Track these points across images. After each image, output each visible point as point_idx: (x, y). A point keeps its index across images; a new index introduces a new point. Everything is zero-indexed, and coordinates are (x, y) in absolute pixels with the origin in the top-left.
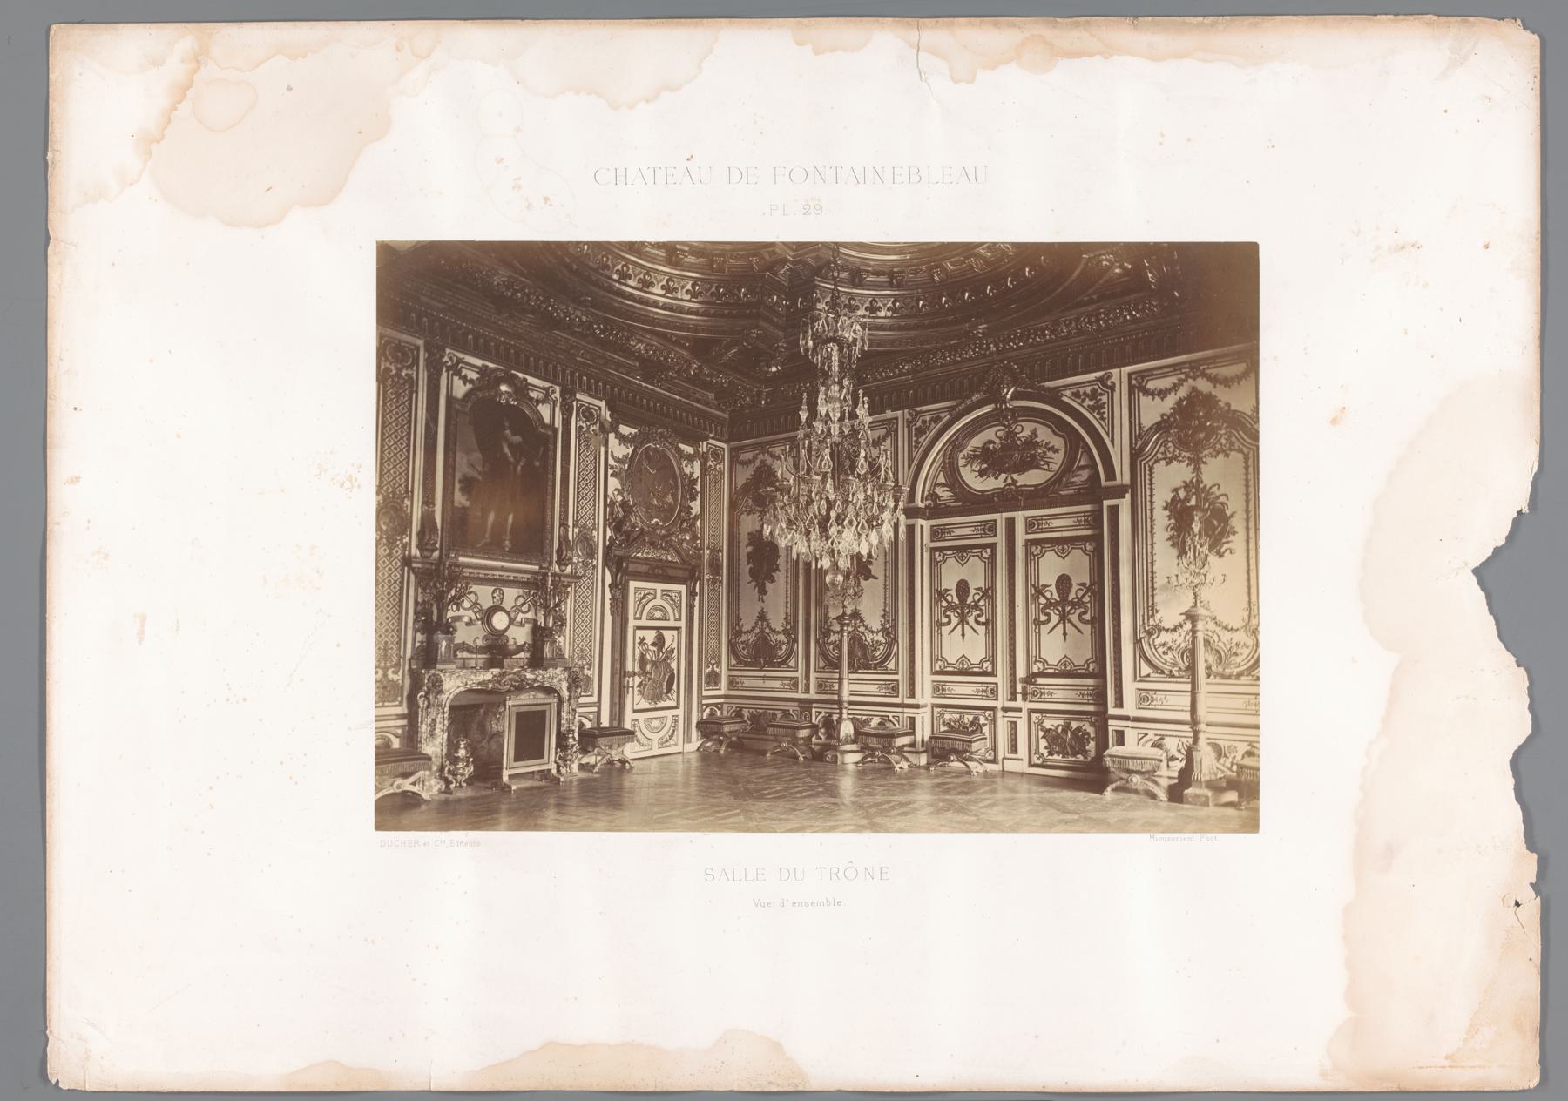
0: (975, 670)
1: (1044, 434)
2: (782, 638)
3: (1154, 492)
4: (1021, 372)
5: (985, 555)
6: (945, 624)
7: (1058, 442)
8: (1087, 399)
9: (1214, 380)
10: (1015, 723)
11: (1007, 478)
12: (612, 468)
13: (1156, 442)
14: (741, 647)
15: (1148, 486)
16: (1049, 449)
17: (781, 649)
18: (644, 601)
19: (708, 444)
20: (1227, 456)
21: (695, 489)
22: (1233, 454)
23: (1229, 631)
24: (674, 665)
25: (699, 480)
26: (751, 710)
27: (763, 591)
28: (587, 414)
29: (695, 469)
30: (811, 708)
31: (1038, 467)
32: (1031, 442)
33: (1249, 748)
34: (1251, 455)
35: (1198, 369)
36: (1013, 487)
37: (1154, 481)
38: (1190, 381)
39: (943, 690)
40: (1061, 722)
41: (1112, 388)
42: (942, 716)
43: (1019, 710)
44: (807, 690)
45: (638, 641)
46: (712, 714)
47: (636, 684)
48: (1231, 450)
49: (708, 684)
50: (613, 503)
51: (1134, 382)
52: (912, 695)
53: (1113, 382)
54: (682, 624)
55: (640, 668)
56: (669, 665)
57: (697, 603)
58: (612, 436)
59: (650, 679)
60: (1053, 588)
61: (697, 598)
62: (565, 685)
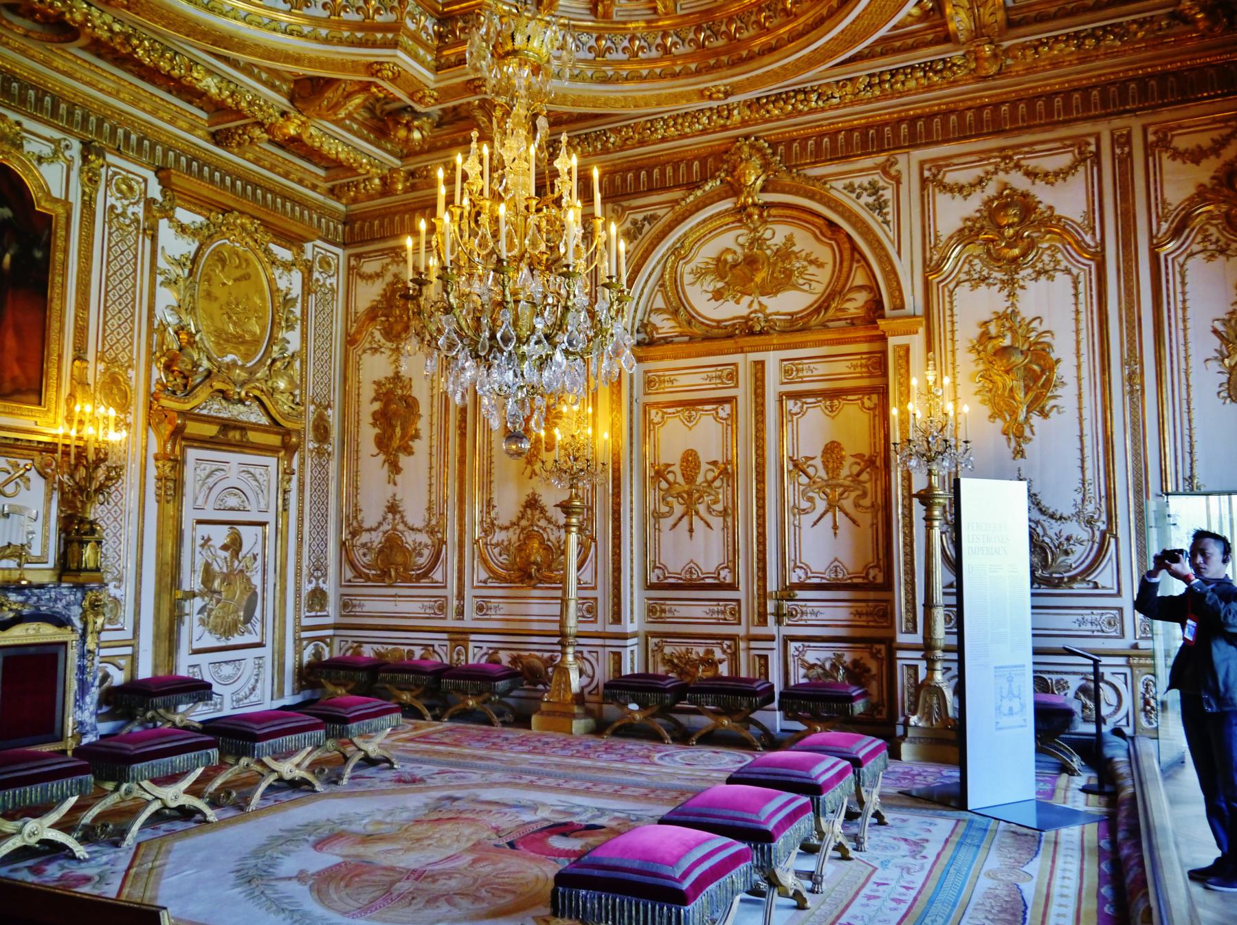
0: (708, 581)
1: (804, 242)
2: (424, 538)
3: (956, 327)
4: (774, 154)
5: (722, 414)
6: (664, 516)
7: (824, 253)
8: (865, 194)
9: (1031, 174)
10: (765, 658)
11: (752, 302)
12: (163, 273)
13: (958, 258)
14: (361, 552)
15: (948, 319)
16: (811, 262)
17: (421, 555)
18: (211, 481)
19: (315, 246)
20: (1051, 278)
21: (292, 312)
22: (1058, 274)
23: (1057, 520)
24: (256, 580)
25: (300, 300)
26: (375, 647)
27: (395, 468)
28: (124, 187)
29: (292, 282)
30: (467, 640)
31: (795, 287)
32: (785, 253)
33: (1084, 682)
34: (1081, 278)
35: (1011, 158)
36: (759, 315)
37: (956, 310)
38: (1001, 174)
39: (663, 611)
40: (830, 654)
41: (898, 182)
42: (660, 648)
43: (772, 639)
44: (460, 613)
45: (199, 541)
46: (317, 654)
47: (196, 609)
48: (1055, 269)
49: (311, 608)
50: (164, 327)
51: (926, 174)
52: (617, 618)
53: (899, 172)
54: (270, 517)
55: (203, 583)
56: (248, 580)
57: (294, 484)
58: (163, 224)
59: (218, 601)
60: (818, 462)
61: (295, 478)
62: (76, 611)
